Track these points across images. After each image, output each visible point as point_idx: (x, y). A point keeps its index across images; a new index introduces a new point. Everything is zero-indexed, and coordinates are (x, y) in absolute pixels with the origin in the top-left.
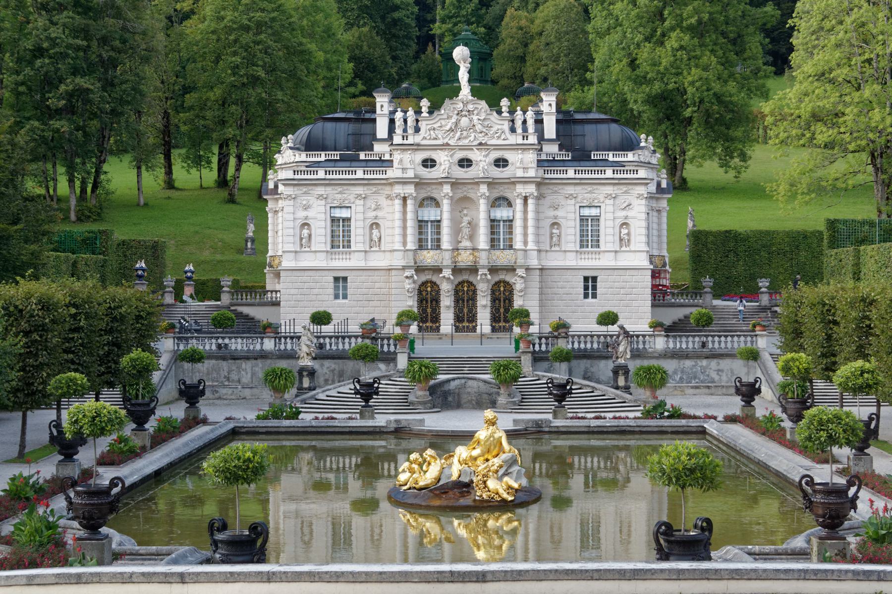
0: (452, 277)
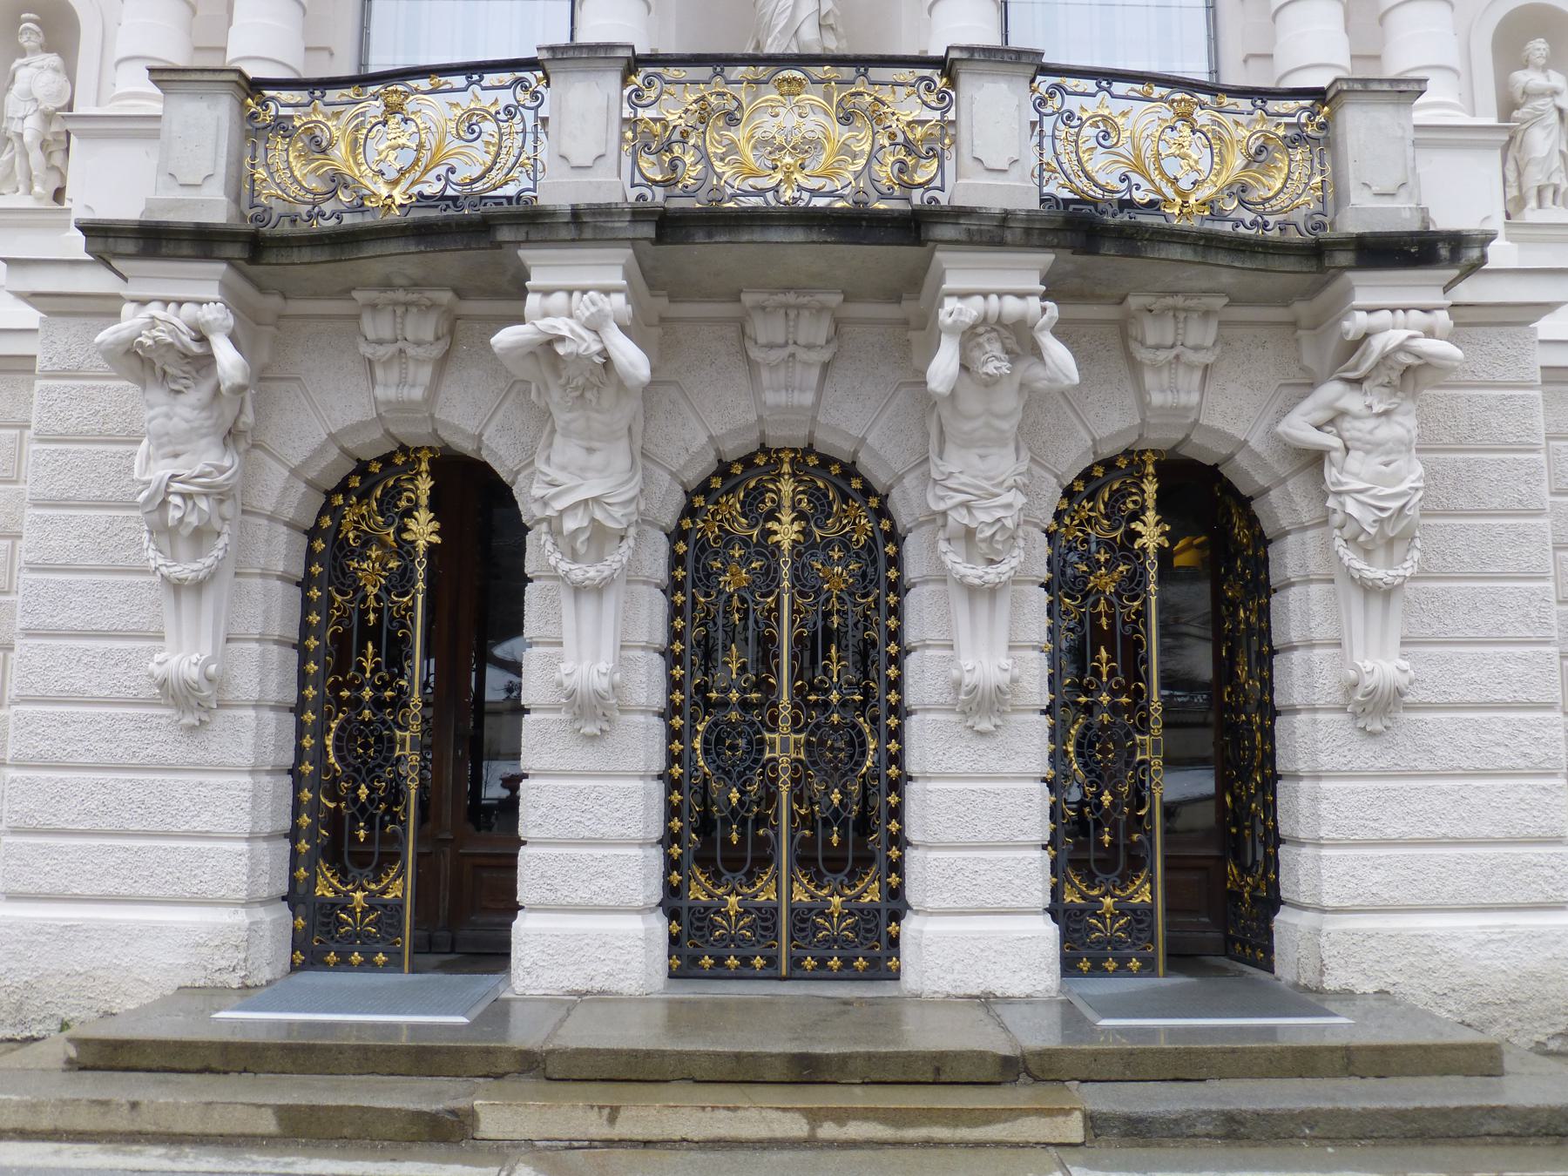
0: (632, 358)
